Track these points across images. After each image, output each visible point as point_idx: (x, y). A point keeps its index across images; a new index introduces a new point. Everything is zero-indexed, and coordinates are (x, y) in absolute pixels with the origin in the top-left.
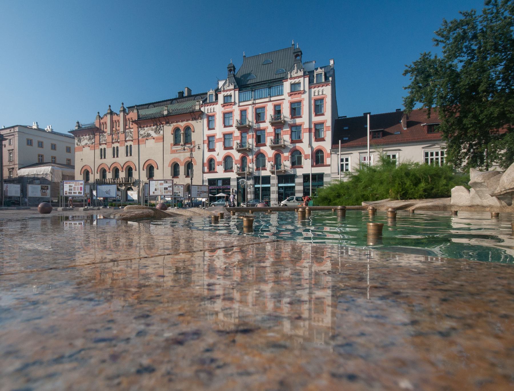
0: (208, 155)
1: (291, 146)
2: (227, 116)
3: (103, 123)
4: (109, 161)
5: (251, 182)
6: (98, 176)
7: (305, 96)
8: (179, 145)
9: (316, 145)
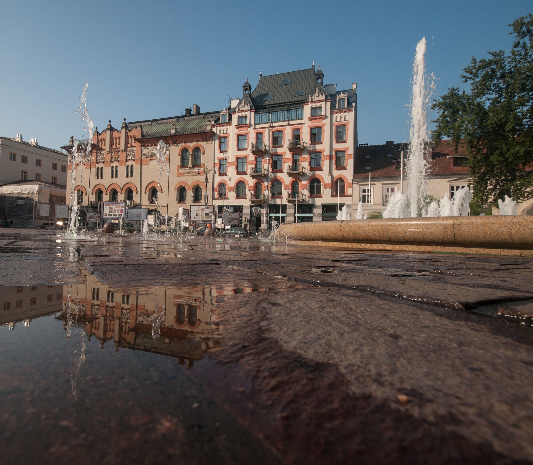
0: (218, 179)
1: (310, 174)
2: (241, 138)
3: (101, 140)
4: (107, 181)
5: (264, 211)
6: (93, 198)
7: (327, 122)
8: (187, 167)
9: (336, 173)
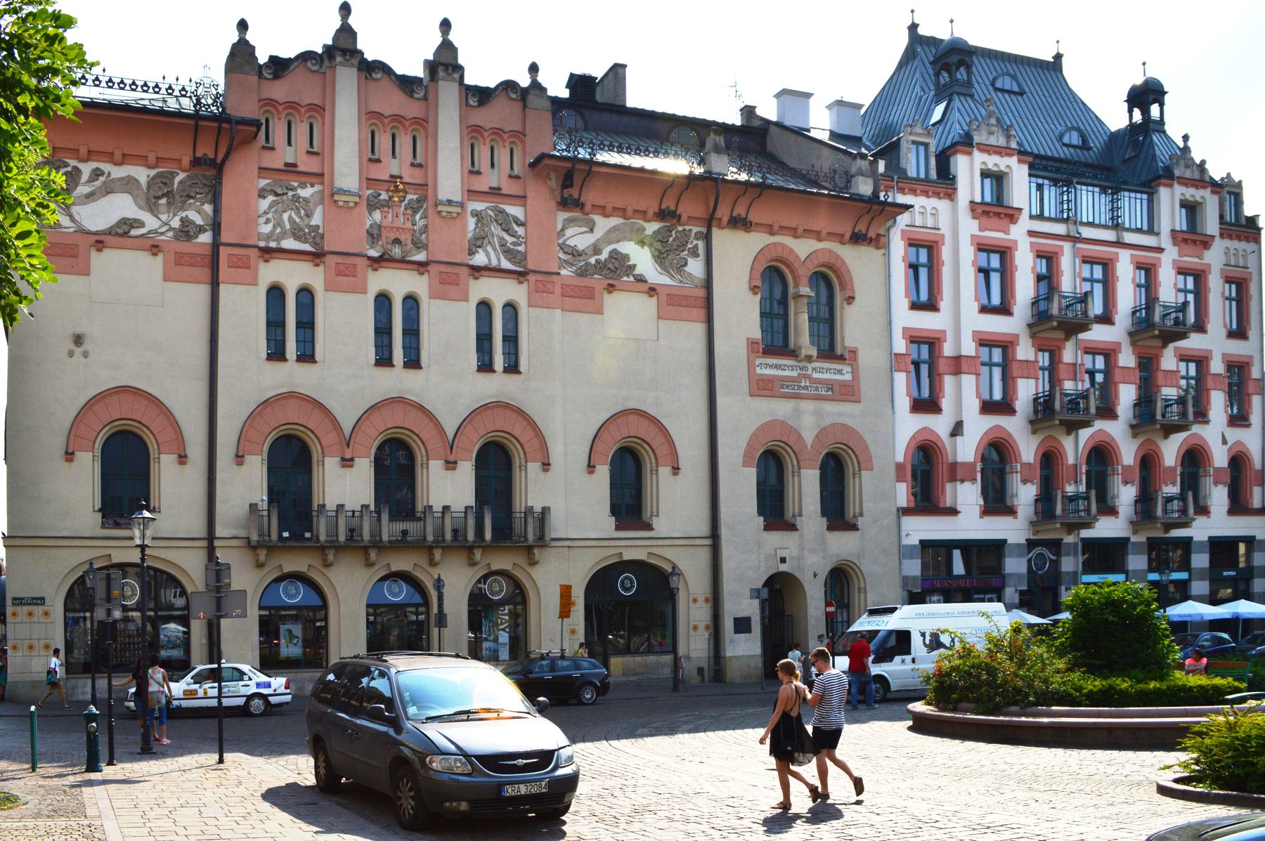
0: (907, 426)
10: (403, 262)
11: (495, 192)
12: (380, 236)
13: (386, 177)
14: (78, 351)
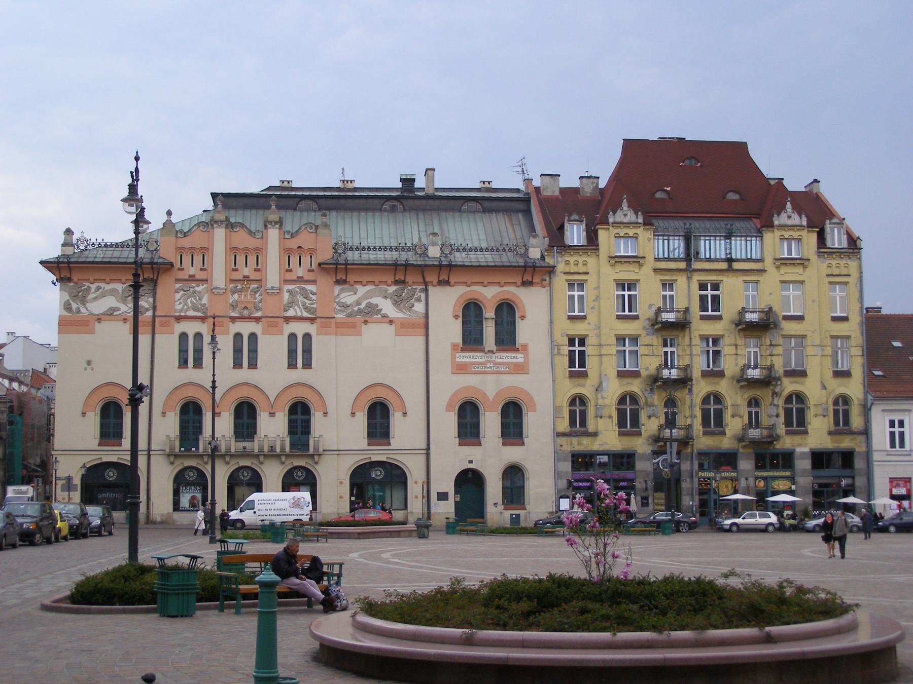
10: (249, 318)
11: (300, 280)
12: (237, 306)
13: (241, 278)
14: (89, 368)
